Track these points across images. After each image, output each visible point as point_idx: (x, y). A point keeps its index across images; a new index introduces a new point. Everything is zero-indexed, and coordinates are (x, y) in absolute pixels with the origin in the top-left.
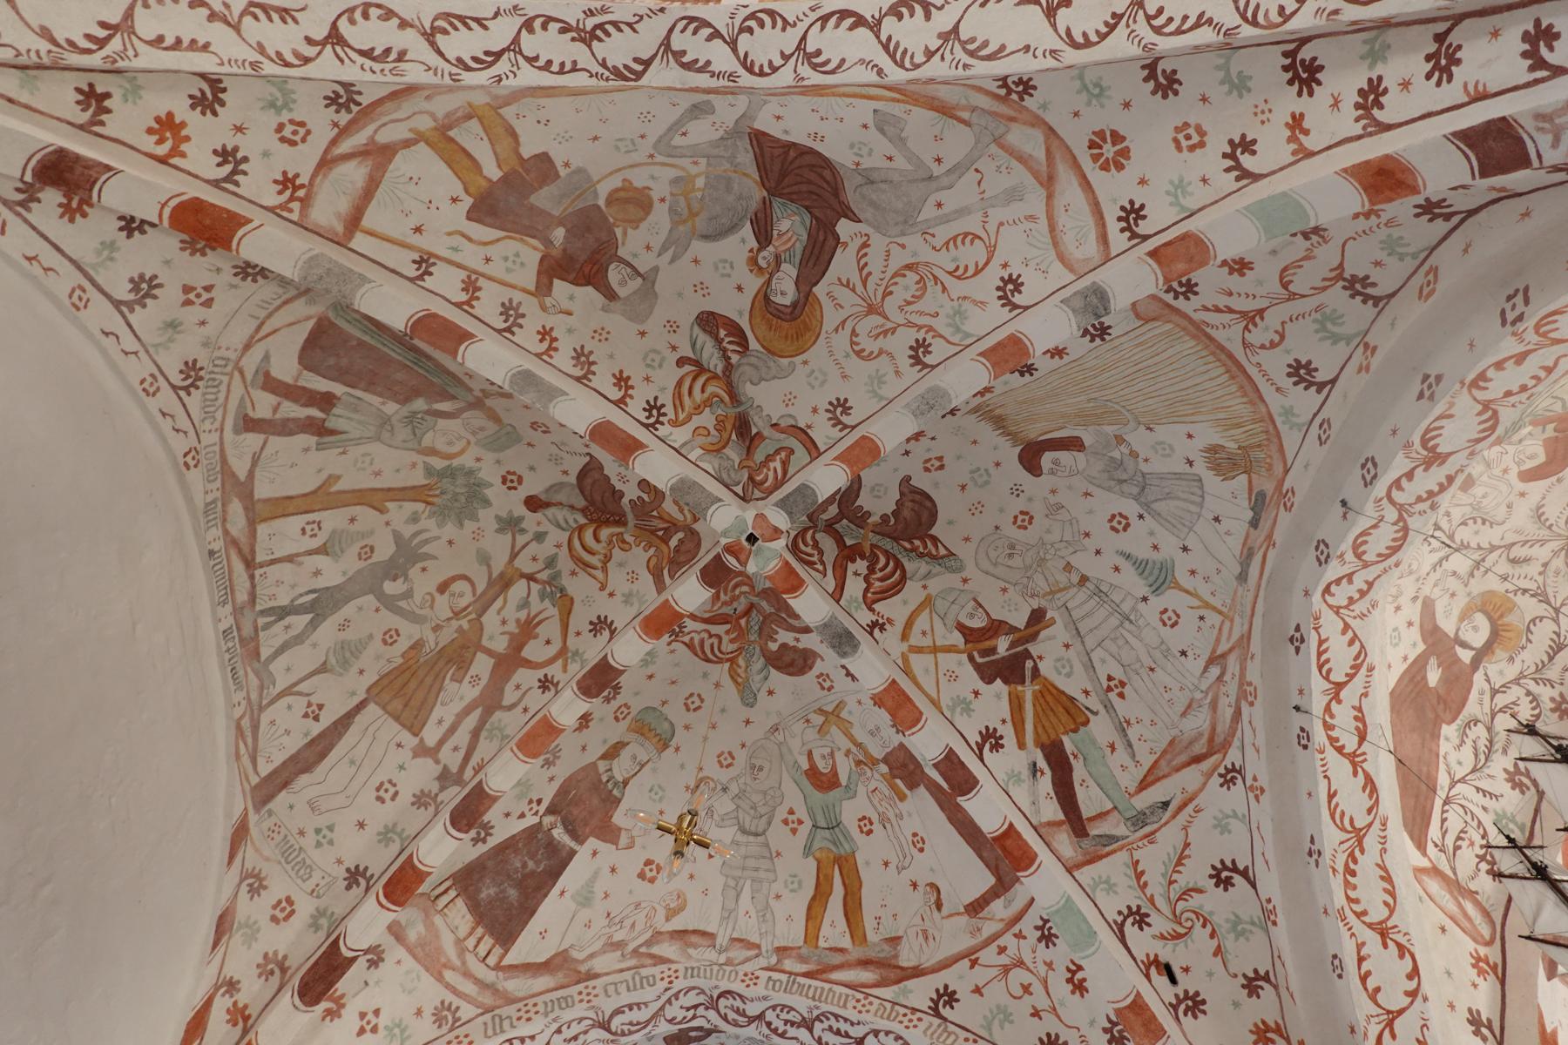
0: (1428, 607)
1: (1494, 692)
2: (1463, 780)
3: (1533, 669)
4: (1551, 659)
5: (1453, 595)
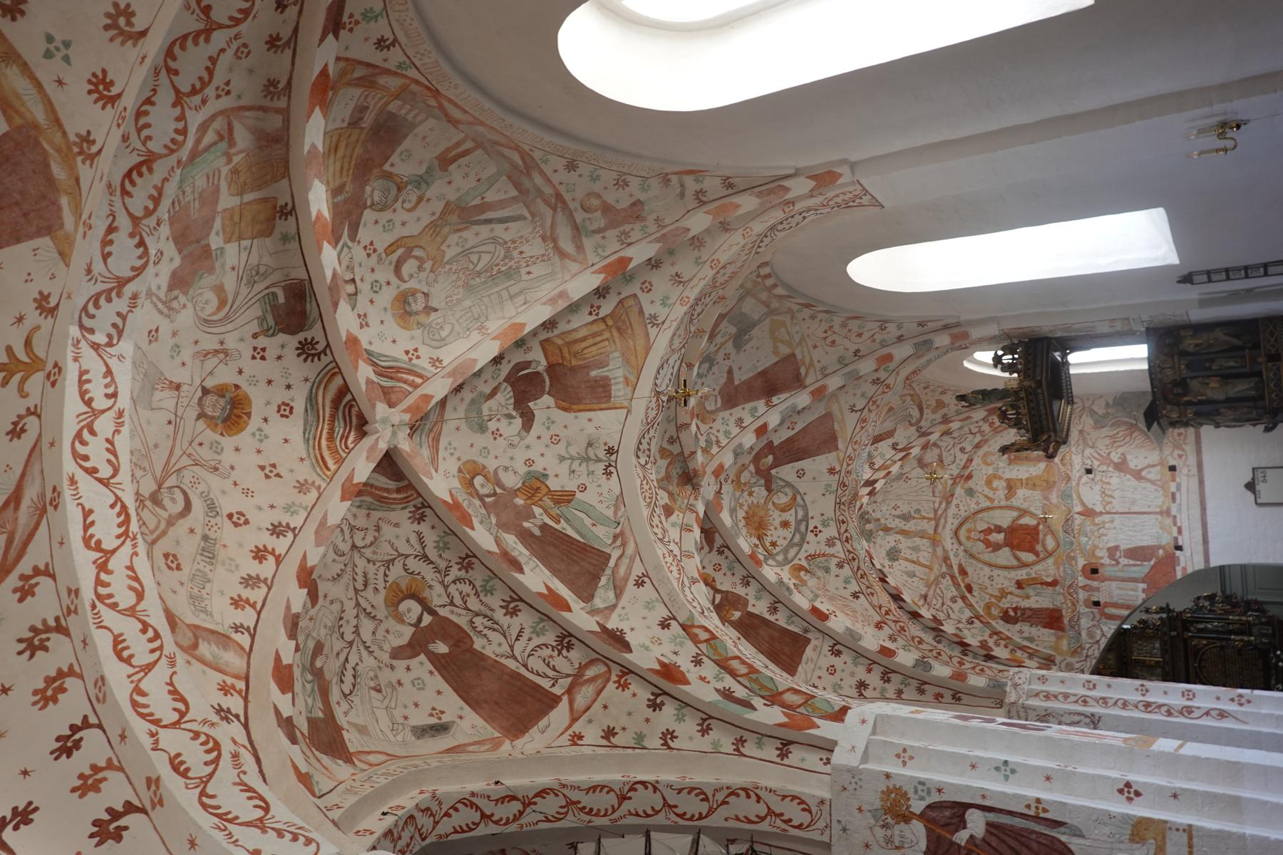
0: (397, 653)
1: (452, 603)
2: (512, 647)
4: (432, 563)
5: (387, 631)
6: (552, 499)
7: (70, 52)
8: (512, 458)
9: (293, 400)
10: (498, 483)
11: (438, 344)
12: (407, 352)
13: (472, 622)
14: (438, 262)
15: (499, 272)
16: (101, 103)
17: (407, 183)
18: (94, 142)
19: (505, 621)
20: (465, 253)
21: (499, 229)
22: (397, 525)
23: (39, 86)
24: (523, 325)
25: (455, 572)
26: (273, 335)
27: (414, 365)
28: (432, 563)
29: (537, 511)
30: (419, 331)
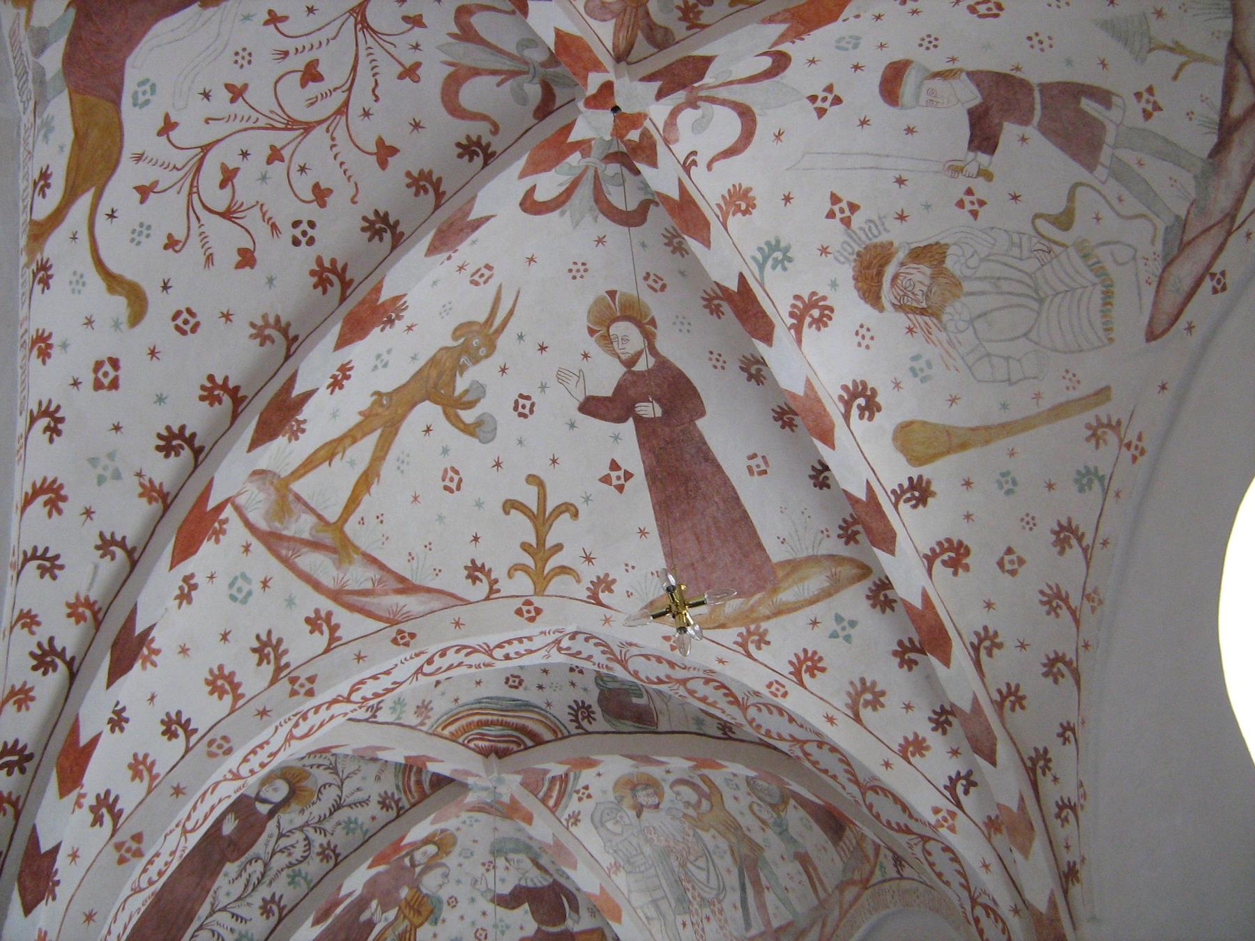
1: (281, 836)
2: (224, 909)
3: (316, 820)
4: (331, 814)
6: (405, 932)
7: (840, 639)
8: (459, 882)
9: (525, 689)
10: (428, 868)
11: (597, 819)
12: (586, 788)
13: (257, 859)
14: (698, 823)
15: (686, 890)
16: (795, 661)
17: (779, 815)
18: (759, 648)
19: (256, 900)
20: (707, 854)
21: (735, 897)
22: (378, 778)
23: (813, 601)
24: (618, 919)
25: (318, 840)
26: (597, 684)
27: (570, 797)
28: (331, 814)
29: (391, 914)
30: (612, 799)
